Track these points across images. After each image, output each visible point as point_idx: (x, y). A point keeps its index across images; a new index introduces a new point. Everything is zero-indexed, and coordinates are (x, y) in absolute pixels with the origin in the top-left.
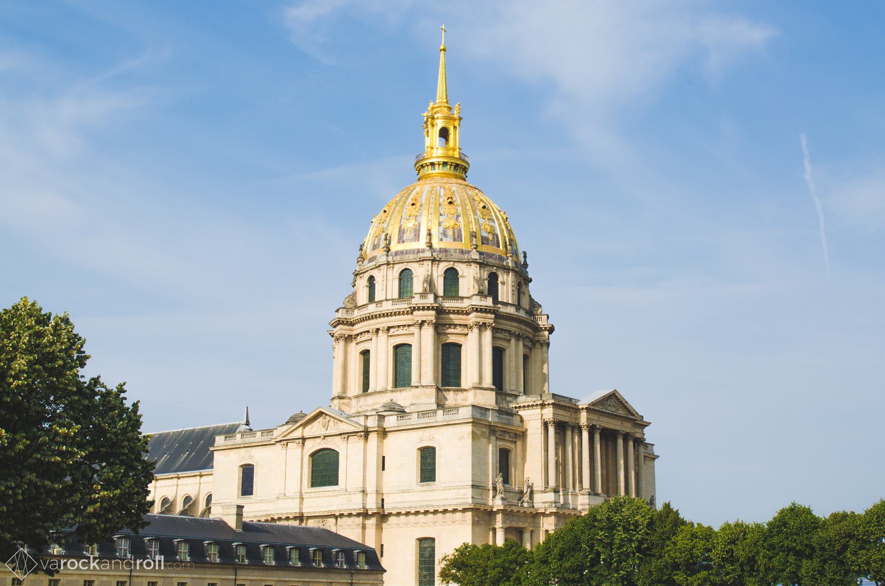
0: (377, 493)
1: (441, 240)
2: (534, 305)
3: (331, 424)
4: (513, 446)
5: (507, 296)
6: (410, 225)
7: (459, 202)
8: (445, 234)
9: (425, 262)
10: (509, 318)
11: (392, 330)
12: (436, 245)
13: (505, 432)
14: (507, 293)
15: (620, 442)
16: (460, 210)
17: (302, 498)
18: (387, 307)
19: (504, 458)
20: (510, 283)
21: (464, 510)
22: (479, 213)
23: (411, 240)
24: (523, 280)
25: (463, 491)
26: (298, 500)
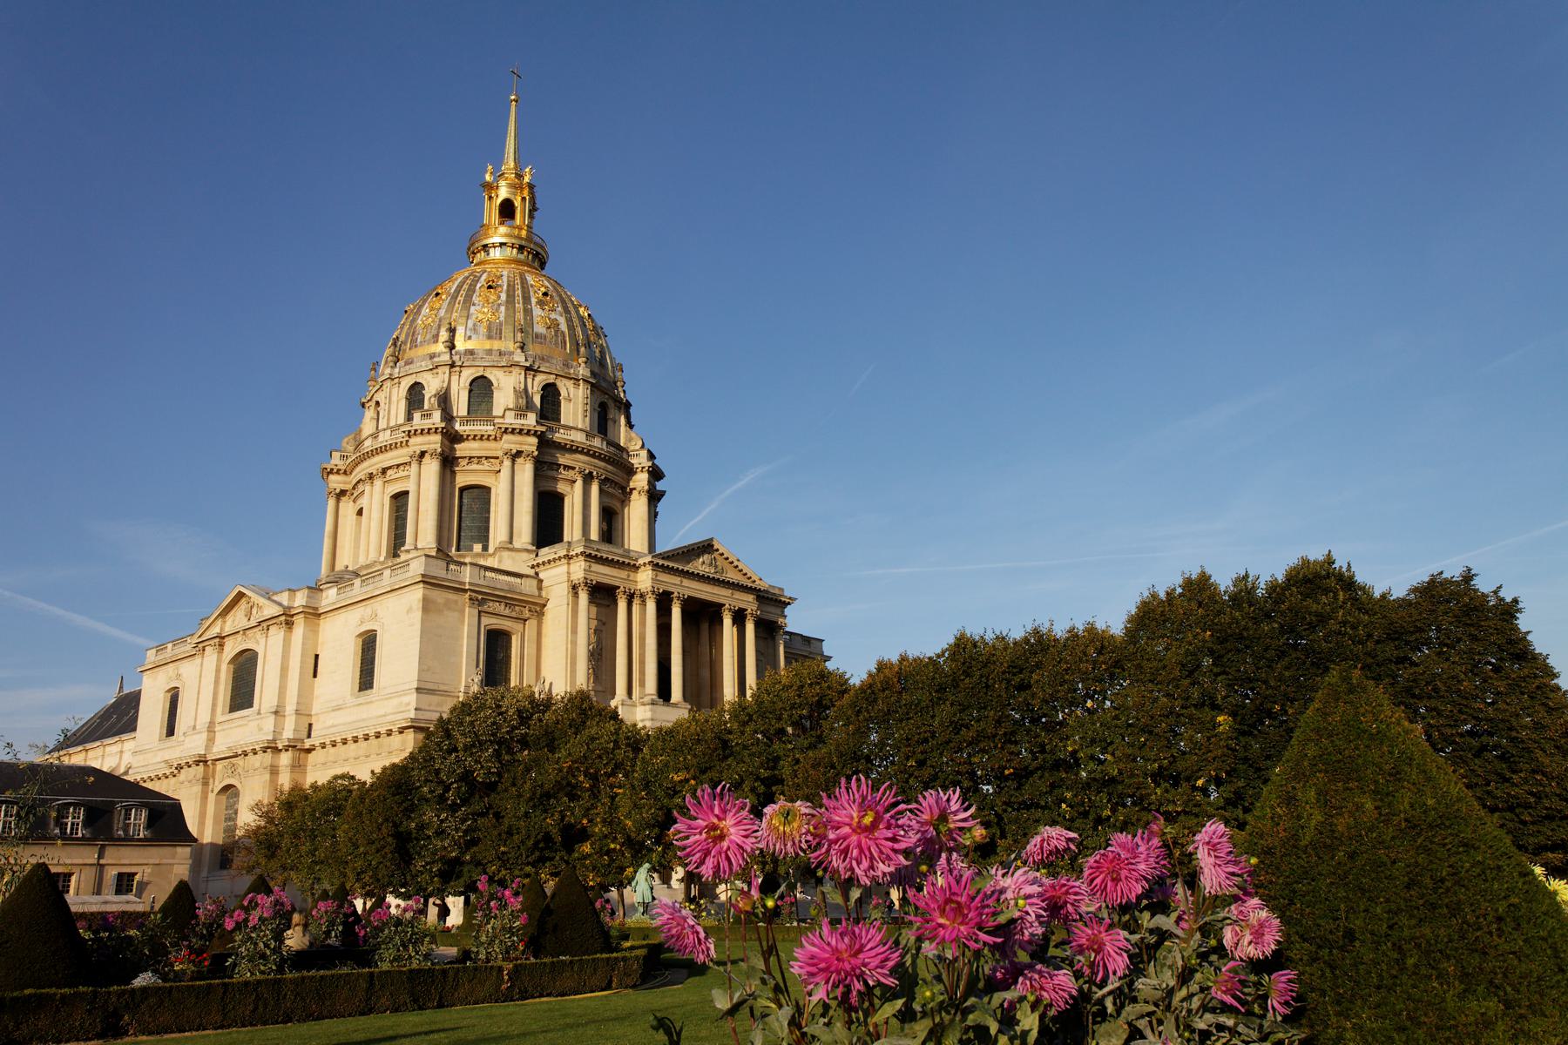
4: (517, 627)
5: (575, 419)
8: (475, 329)
9: (440, 370)
10: (572, 449)
11: (389, 472)
12: (461, 345)
14: (575, 414)
15: (727, 621)
16: (504, 296)
18: (385, 438)
21: (402, 731)
22: (534, 300)
24: (609, 404)
25: (406, 699)
26: (205, 736)
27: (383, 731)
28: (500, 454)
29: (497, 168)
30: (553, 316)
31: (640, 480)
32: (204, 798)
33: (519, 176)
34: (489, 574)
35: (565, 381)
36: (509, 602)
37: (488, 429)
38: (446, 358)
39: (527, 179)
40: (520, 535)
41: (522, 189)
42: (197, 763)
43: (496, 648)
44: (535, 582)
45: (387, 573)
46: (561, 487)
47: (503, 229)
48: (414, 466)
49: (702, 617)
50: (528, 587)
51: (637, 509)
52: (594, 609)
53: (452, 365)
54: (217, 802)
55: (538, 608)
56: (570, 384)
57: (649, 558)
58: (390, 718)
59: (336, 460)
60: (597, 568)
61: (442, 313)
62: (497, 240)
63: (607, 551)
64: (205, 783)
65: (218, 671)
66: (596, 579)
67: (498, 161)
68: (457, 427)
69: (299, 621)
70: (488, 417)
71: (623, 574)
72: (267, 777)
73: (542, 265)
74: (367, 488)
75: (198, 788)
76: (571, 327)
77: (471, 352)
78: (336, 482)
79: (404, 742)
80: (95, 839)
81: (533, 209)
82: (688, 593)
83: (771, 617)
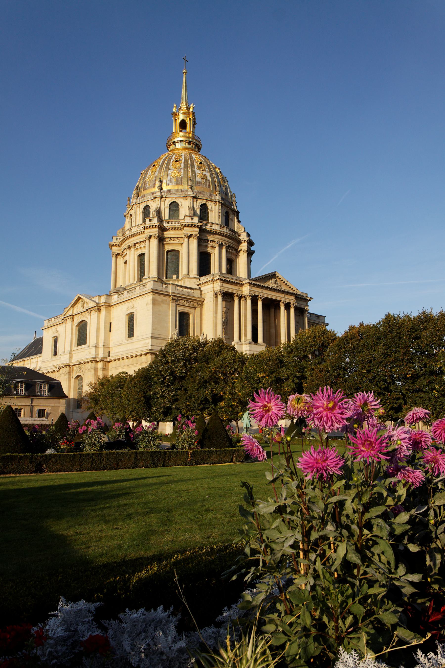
0: (104, 346)
1: (169, 185)
3: (85, 304)
5: (215, 220)
7: (183, 161)
8: (171, 181)
9: (157, 199)
11: (137, 245)
12: (165, 188)
14: (215, 217)
15: (282, 308)
16: (183, 165)
17: (71, 353)
18: (134, 230)
20: (217, 211)
21: (146, 354)
22: (196, 166)
24: (229, 212)
26: (68, 355)
27: (138, 354)
28: (183, 236)
29: (178, 105)
30: (204, 173)
31: (244, 246)
32: (70, 380)
33: (188, 109)
34: (180, 288)
35: (210, 202)
36: (188, 300)
37: (178, 225)
38: (159, 194)
39: (191, 110)
40: (192, 272)
41: (189, 114)
42: (66, 366)
43: (183, 320)
44: (199, 292)
45: (138, 288)
46: (210, 250)
47: (181, 134)
49: (271, 306)
50: (196, 294)
51: (242, 259)
52: (224, 303)
53: (162, 197)
54: (75, 382)
55: (201, 303)
56: (212, 204)
57: (248, 281)
58: (141, 349)
59: (115, 241)
61: (156, 174)
62: (179, 139)
63: (230, 278)
64: (70, 375)
65: (72, 329)
66: (225, 290)
67: (178, 102)
68: (165, 224)
69: (103, 309)
71: (236, 288)
72: (93, 372)
73: (199, 150)
74: (128, 252)
75: (67, 376)
76: (212, 178)
77: (169, 191)
78: (115, 250)
79: (147, 359)
81: (195, 124)
82: (265, 296)
83: (302, 306)
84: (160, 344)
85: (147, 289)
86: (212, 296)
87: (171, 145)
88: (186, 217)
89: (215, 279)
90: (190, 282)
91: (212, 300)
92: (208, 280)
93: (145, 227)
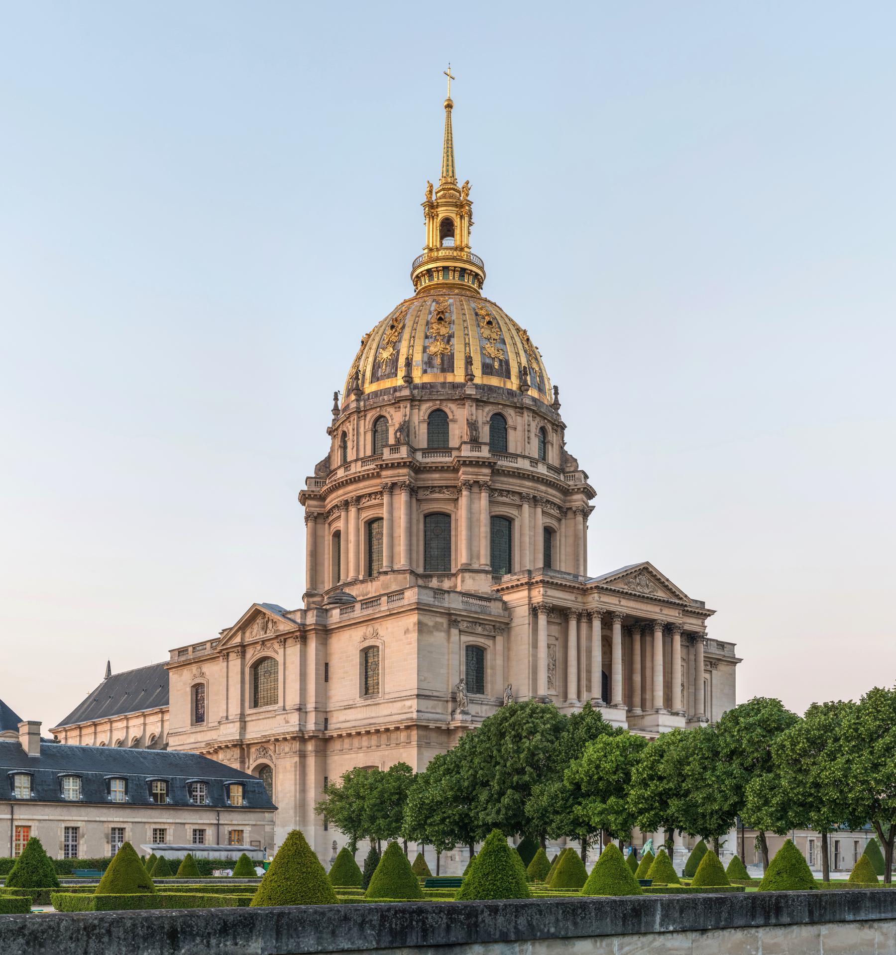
1: (425, 372)
2: (567, 459)
4: (489, 642)
6: (385, 355)
8: (429, 363)
13: (476, 622)
19: (476, 658)
23: (388, 376)
25: (408, 703)
40: (478, 558)
44: (500, 605)
45: (384, 599)
48: (386, 498)
50: (495, 608)
60: (551, 592)
70: (448, 450)
79: (409, 737)
80: (216, 807)
84: (433, 708)
85: (405, 602)
86: (527, 614)
87: (423, 275)
88: (463, 446)
89: (534, 581)
90: (474, 579)
91: (527, 622)
92: (519, 583)
93: (381, 465)
